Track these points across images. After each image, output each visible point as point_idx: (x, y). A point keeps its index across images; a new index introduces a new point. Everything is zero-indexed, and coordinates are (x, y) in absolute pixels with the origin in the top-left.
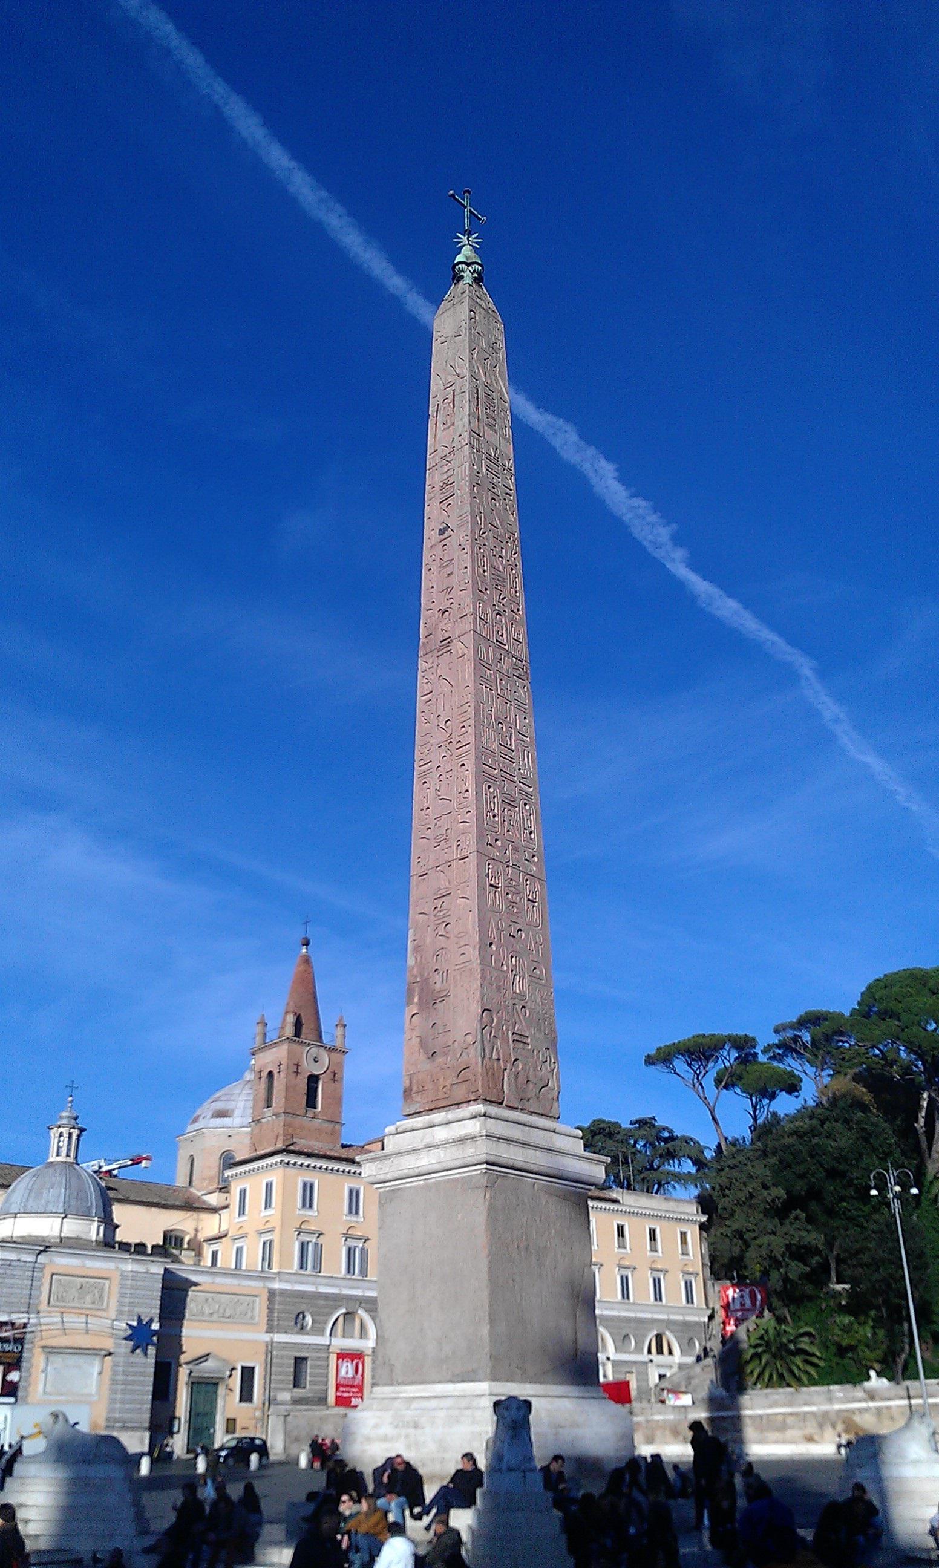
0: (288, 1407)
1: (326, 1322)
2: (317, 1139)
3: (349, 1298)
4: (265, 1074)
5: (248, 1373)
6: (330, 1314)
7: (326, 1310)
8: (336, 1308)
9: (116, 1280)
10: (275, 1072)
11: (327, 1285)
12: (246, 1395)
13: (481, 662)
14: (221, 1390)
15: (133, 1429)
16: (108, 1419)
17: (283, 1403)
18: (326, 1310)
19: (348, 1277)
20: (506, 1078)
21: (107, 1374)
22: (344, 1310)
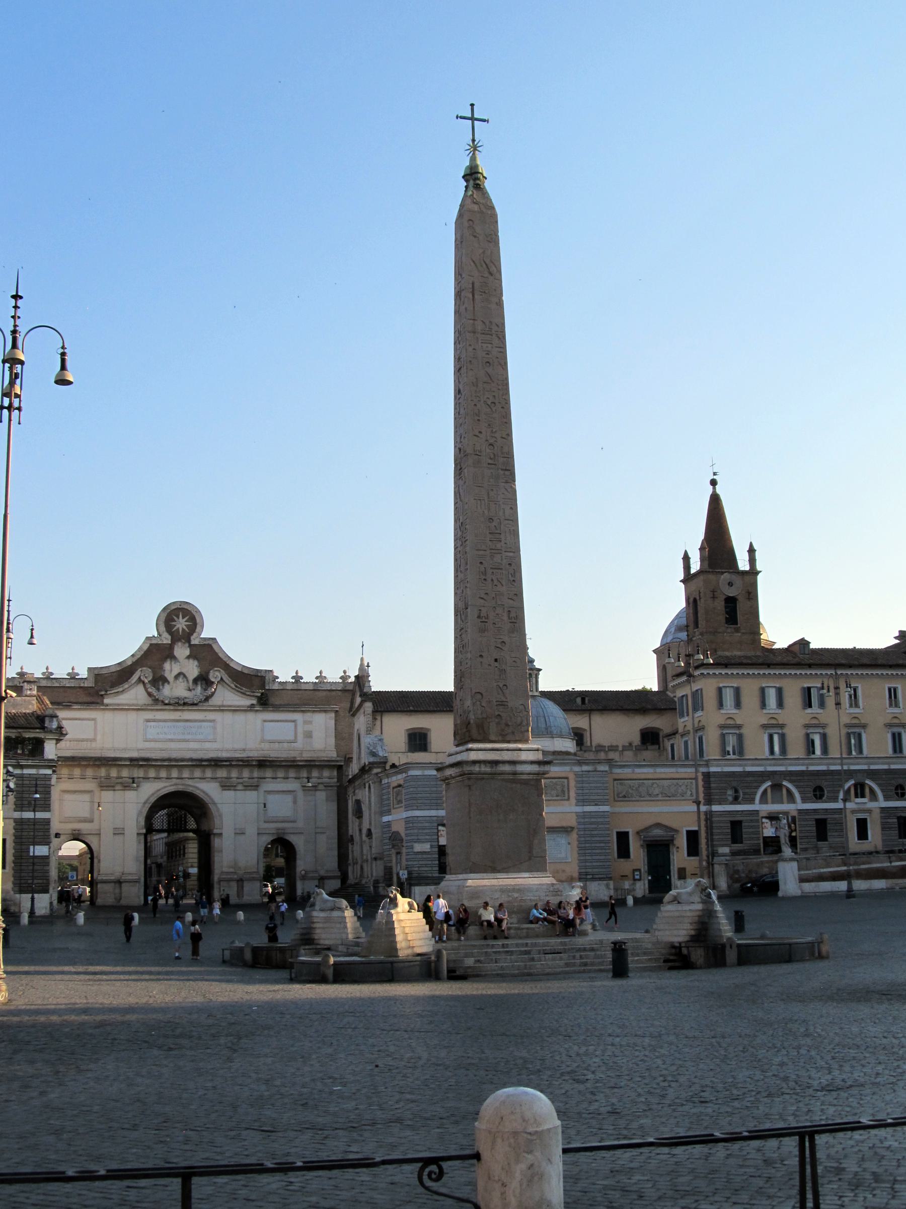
0: (728, 858)
1: (755, 794)
2: (740, 650)
3: (774, 773)
4: (691, 600)
5: (693, 837)
6: (758, 787)
7: (755, 784)
8: (764, 782)
9: (572, 777)
10: (698, 598)
11: (753, 765)
12: (693, 850)
14: (673, 850)
15: (600, 879)
16: (580, 873)
17: (724, 855)
18: (755, 784)
19: (771, 757)
21: (575, 843)
22: (769, 783)
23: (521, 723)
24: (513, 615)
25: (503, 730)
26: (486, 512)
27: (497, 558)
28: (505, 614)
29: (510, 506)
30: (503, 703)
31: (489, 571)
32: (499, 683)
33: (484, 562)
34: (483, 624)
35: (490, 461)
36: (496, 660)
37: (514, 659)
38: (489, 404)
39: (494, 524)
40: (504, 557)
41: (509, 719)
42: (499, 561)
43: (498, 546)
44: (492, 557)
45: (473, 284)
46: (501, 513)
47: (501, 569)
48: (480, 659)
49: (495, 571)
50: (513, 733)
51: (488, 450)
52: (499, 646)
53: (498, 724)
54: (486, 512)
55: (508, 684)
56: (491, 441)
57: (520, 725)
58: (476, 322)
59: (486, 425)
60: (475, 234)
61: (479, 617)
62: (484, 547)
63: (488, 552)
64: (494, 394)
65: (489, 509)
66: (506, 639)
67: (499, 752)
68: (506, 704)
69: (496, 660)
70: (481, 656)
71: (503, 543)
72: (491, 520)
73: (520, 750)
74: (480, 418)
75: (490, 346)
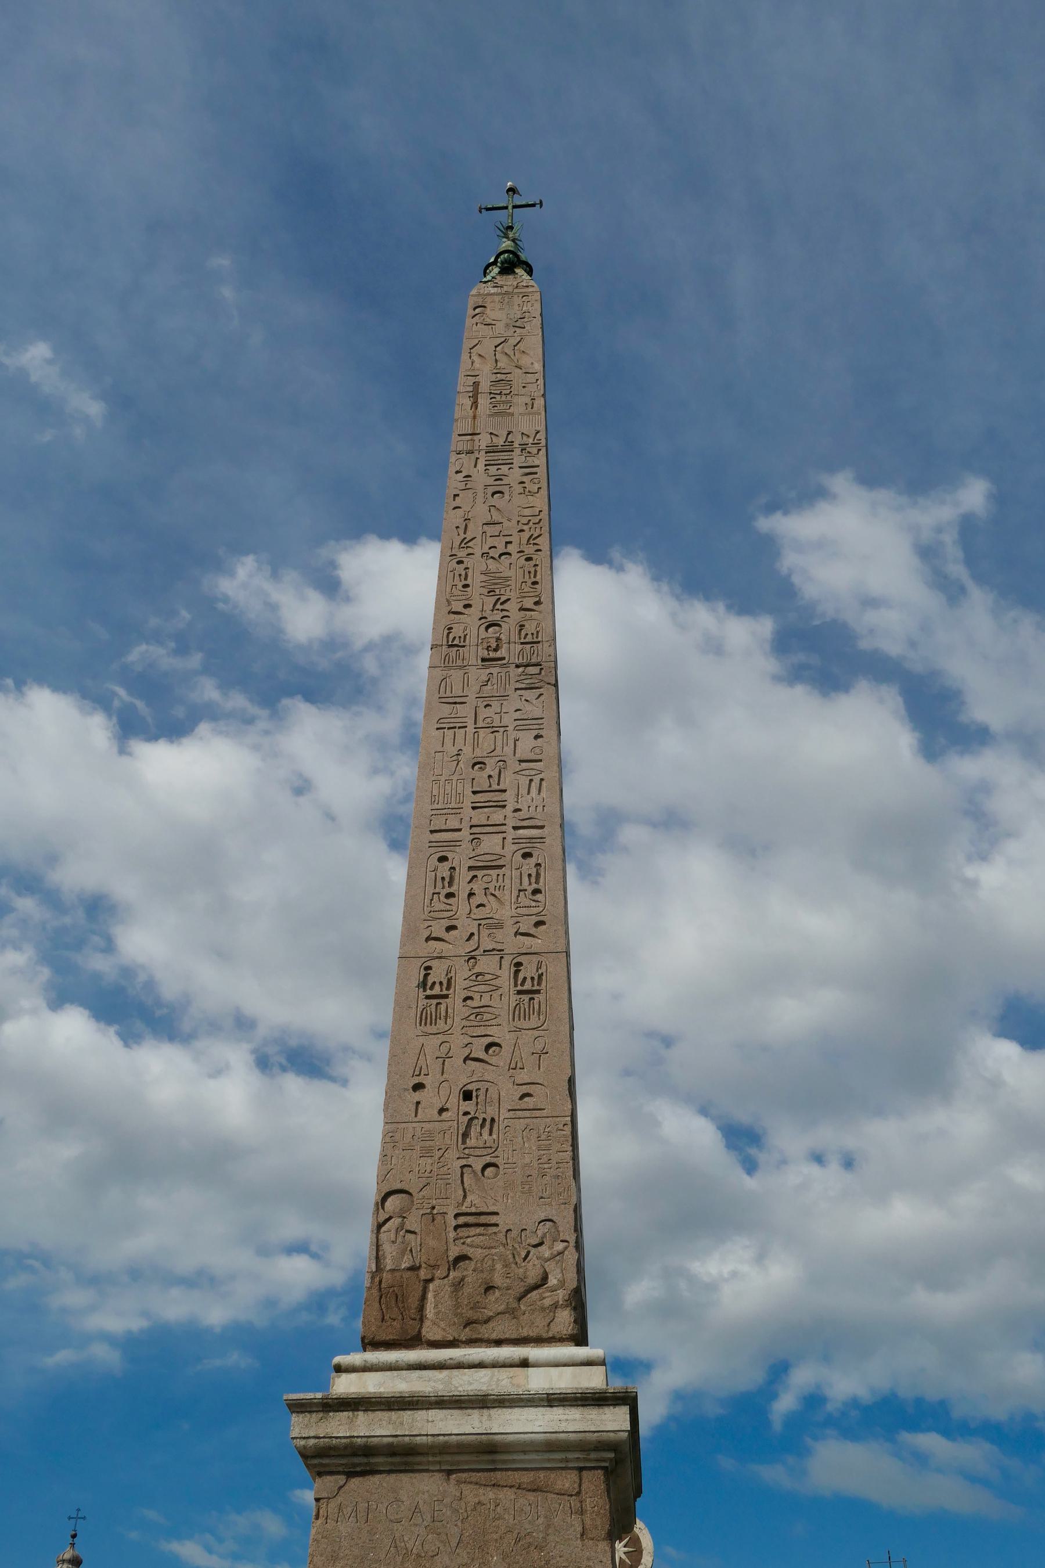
13: (443, 700)
20: (430, 1296)
23: (545, 1279)
24: (529, 970)
25: (475, 1307)
26: (467, 750)
27: (491, 844)
28: (506, 973)
29: (535, 733)
30: (483, 1219)
31: (463, 876)
32: (471, 1161)
33: (450, 855)
34: (434, 1002)
35: (492, 655)
36: (467, 1096)
37: (525, 1089)
38: (497, 556)
39: (488, 771)
40: (509, 840)
41: (499, 1266)
42: (498, 849)
43: (497, 817)
44: (475, 839)
45: (476, 385)
46: (509, 750)
47: (501, 867)
48: (417, 1096)
49: (480, 873)
50: (511, 1312)
51: (483, 634)
52: (482, 1055)
53: (458, 1285)
54: (467, 750)
55: (499, 1161)
56: (496, 617)
57: (536, 1287)
58: (476, 438)
59: (485, 591)
60: (489, 321)
61: (423, 985)
62: (453, 823)
63: (465, 834)
64: (508, 539)
65: (476, 744)
66: (497, 1033)
67: (445, 1373)
68: (493, 1219)
69: (467, 1096)
70: (418, 1087)
71: (510, 807)
72: (478, 764)
73: (525, 1364)
74: (469, 581)
75: (505, 468)
